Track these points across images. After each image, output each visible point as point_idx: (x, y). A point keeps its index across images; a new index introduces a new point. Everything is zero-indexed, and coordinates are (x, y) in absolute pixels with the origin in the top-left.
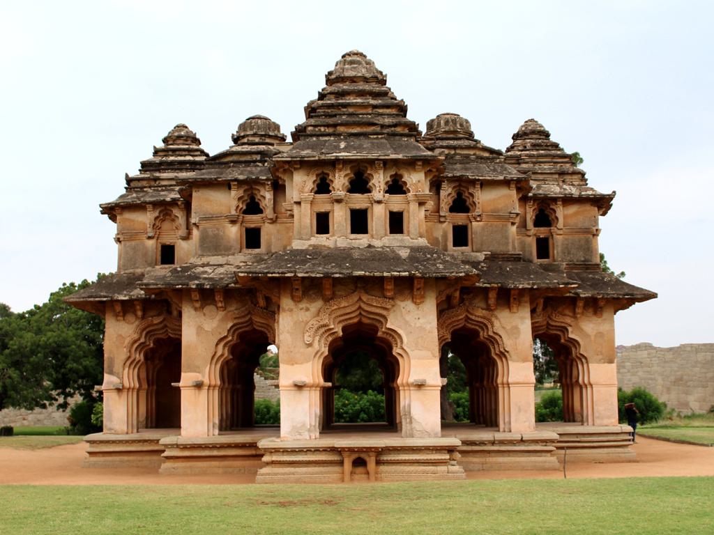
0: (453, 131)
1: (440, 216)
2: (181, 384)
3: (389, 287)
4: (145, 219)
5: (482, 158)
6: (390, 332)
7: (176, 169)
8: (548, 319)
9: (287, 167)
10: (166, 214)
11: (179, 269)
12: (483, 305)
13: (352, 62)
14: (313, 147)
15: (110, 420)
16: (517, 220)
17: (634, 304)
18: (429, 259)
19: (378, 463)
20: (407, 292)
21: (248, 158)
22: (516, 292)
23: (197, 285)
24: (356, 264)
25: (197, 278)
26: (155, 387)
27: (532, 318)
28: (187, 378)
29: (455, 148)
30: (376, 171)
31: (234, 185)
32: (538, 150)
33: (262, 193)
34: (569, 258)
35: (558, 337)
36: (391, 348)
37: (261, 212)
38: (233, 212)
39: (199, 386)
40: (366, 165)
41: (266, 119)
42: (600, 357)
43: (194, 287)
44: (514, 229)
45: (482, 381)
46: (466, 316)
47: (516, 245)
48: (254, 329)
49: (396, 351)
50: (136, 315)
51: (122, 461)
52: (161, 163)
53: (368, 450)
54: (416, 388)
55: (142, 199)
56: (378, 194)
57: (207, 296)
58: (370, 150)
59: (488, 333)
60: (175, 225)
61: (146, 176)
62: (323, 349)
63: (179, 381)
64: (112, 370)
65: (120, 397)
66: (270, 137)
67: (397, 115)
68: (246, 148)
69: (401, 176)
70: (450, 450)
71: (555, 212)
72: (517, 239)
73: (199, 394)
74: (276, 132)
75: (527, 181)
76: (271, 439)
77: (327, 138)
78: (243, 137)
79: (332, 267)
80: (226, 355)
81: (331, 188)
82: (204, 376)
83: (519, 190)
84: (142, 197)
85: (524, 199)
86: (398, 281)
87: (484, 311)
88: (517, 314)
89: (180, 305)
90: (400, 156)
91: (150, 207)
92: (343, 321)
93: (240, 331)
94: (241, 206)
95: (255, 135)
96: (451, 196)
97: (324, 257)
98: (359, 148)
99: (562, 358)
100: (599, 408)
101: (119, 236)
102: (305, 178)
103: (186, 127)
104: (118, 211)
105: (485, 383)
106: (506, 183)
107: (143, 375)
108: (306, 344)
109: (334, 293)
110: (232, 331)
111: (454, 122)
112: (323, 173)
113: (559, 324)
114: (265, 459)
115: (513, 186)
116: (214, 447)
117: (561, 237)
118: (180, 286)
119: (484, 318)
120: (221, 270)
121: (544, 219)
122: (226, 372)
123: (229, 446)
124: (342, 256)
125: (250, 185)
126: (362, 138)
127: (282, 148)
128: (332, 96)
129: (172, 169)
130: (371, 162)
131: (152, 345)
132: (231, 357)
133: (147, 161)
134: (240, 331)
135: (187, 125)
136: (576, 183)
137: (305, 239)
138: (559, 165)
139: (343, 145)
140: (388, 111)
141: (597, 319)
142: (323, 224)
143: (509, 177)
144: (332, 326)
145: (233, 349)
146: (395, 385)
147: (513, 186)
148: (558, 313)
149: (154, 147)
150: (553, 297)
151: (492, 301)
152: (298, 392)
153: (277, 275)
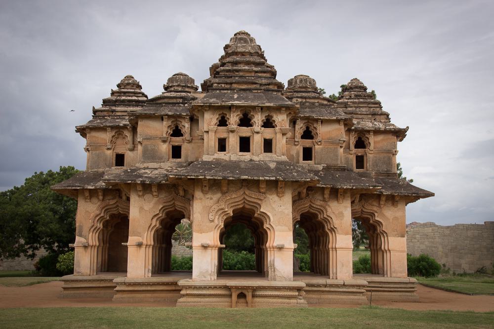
0: (304, 87)
1: (295, 141)
2: (128, 244)
3: (262, 186)
4: (106, 136)
5: (323, 105)
6: (262, 214)
7: (126, 105)
8: (362, 208)
9: (200, 108)
10: (119, 134)
11: (129, 171)
12: (321, 198)
13: (241, 39)
14: (217, 97)
15: (79, 266)
16: (344, 145)
17: (419, 199)
18: (288, 169)
19: (254, 296)
20: (274, 189)
21: (174, 101)
22: (342, 191)
23: (141, 181)
24: (243, 171)
25: (141, 177)
26: (108, 245)
27: (352, 208)
28: (132, 240)
29: (305, 98)
30: (256, 113)
31: (166, 118)
32: (358, 99)
34: (376, 169)
35: (368, 219)
36: (262, 224)
37: (182, 135)
38: (165, 135)
39: (140, 245)
40: (250, 109)
41: (186, 75)
42: (396, 233)
43: (139, 182)
44: (342, 150)
45: (319, 246)
46: (310, 205)
47: (343, 161)
48: (176, 209)
49: (266, 226)
50: (98, 199)
51: (85, 293)
52: (116, 101)
53: (247, 288)
54: (278, 250)
55: (104, 124)
56: (257, 127)
57: (147, 188)
58: (253, 100)
59: (323, 216)
60: (125, 141)
61: (107, 109)
62: (220, 224)
63: (127, 241)
64: (81, 234)
65: (86, 251)
66: (188, 87)
67: (270, 78)
68: (173, 94)
69: (272, 117)
70: (299, 289)
71: (369, 139)
72: (345, 156)
73: (140, 249)
74: (192, 84)
75: (351, 120)
76: (186, 280)
77: (226, 91)
78: (171, 87)
79: (228, 173)
80: (158, 226)
81: (227, 123)
82: (143, 239)
83: (345, 125)
84: (104, 122)
85: (349, 131)
86: (268, 182)
87: (321, 202)
88: (342, 205)
89: (129, 193)
90: (272, 105)
92: (233, 206)
93: (166, 211)
94: (169, 131)
95: (178, 86)
96: (302, 128)
97: (222, 167)
98: (246, 99)
99: (371, 232)
100: (395, 266)
101: (88, 147)
102: (212, 116)
103: (133, 78)
104: (88, 131)
105: (321, 247)
106: (338, 121)
107: (101, 237)
108: (210, 220)
109: (228, 189)
110: (162, 210)
111: (306, 80)
112: (223, 113)
113: (369, 211)
114: (183, 292)
115: (342, 123)
116: (148, 284)
117: (372, 155)
118: (130, 182)
119: (321, 206)
120: (156, 172)
121: (360, 144)
122: (156, 236)
123: (158, 284)
124: (233, 166)
125: (176, 118)
126: (248, 92)
127: (196, 95)
128: (230, 64)
129: (124, 105)
130: (254, 108)
131: (108, 218)
132: (161, 227)
133: (107, 99)
134: (167, 210)
135: (133, 76)
136: (383, 121)
137: (211, 155)
138: (372, 109)
139: (236, 96)
140: (264, 75)
141: (394, 208)
142: (222, 146)
143: (339, 117)
144: (227, 210)
145: (162, 222)
146: (264, 247)
147: (342, 123)
148: (369, 203)
149: (112, 90)
150: (366, 193)
151: (326, 196)
152: (204, 250)
153: (194, 177)
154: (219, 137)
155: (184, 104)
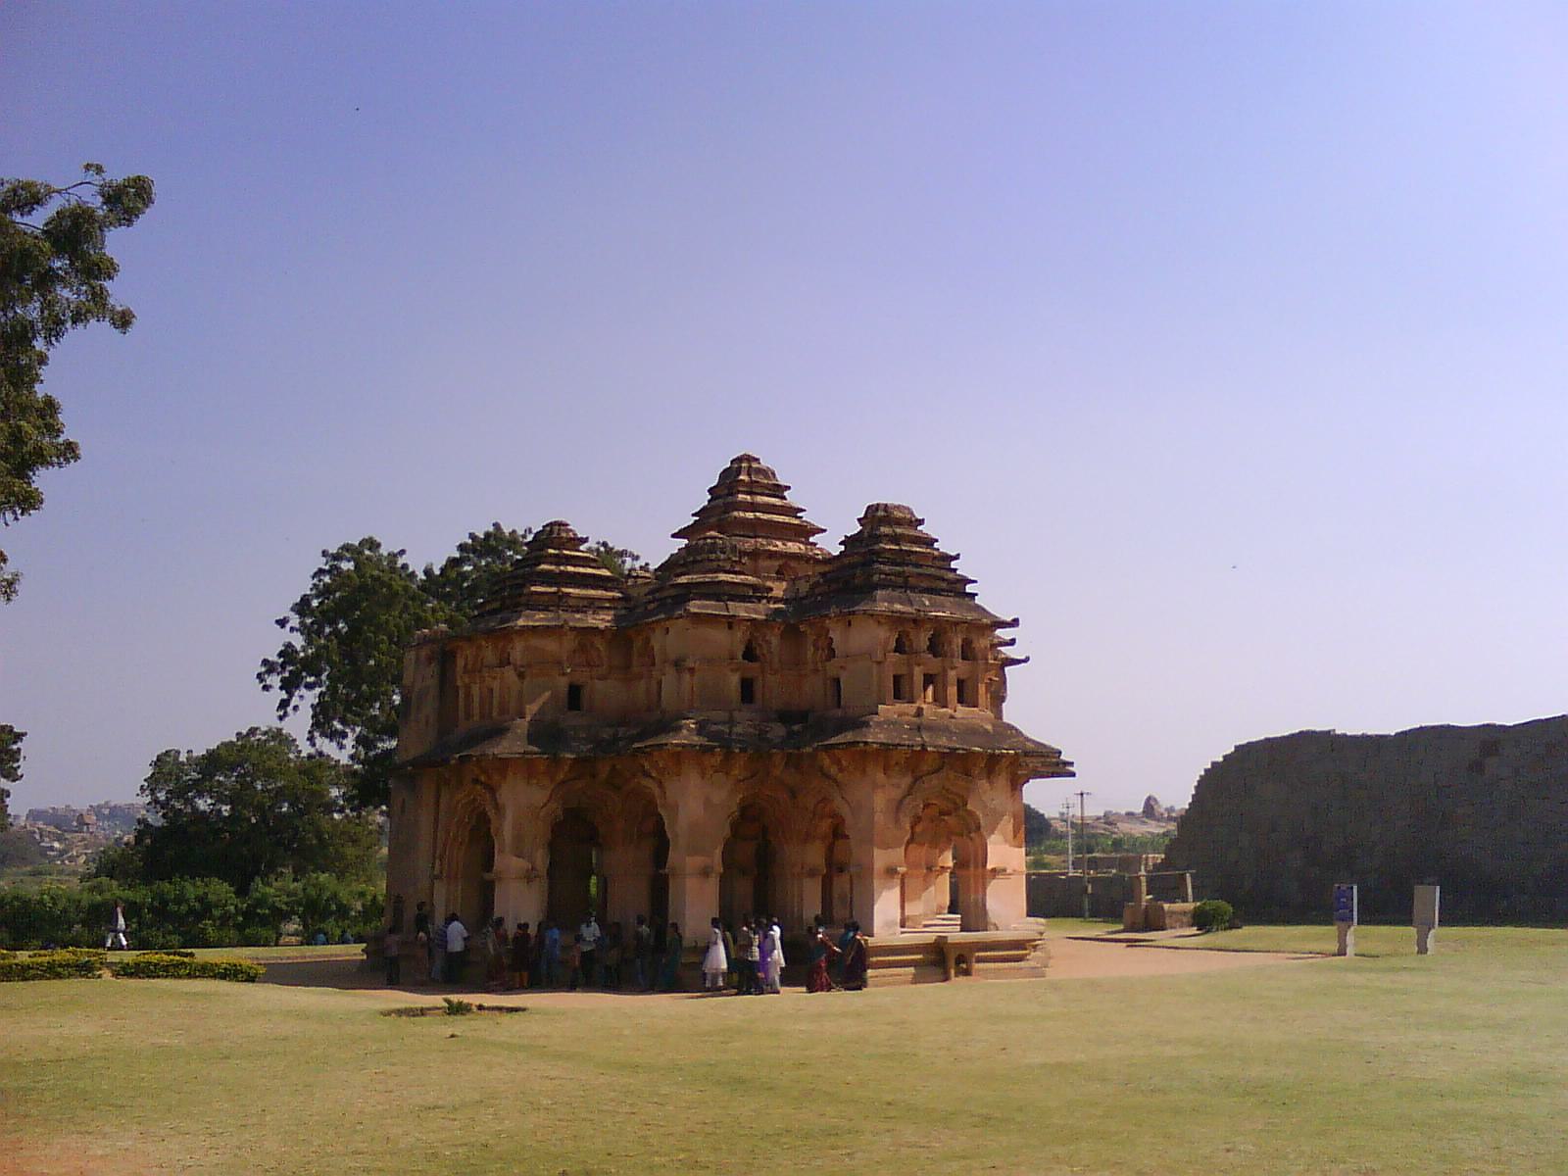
21: (741, 591)
33: (767, 638)
91: (571, 636)
101: (522, 669)
130: (956, 623)
154: (895, 673)
155: (759, 599)
